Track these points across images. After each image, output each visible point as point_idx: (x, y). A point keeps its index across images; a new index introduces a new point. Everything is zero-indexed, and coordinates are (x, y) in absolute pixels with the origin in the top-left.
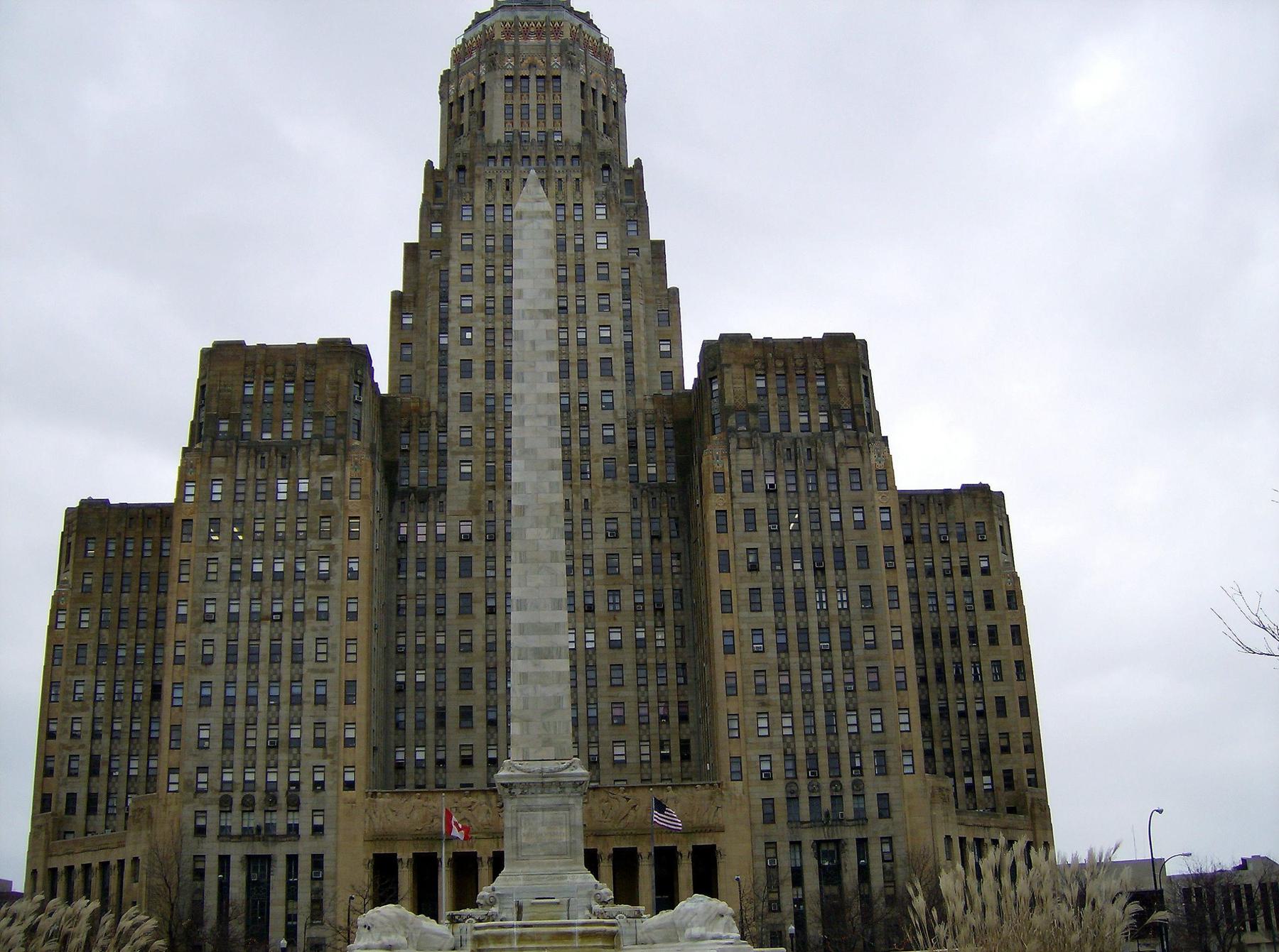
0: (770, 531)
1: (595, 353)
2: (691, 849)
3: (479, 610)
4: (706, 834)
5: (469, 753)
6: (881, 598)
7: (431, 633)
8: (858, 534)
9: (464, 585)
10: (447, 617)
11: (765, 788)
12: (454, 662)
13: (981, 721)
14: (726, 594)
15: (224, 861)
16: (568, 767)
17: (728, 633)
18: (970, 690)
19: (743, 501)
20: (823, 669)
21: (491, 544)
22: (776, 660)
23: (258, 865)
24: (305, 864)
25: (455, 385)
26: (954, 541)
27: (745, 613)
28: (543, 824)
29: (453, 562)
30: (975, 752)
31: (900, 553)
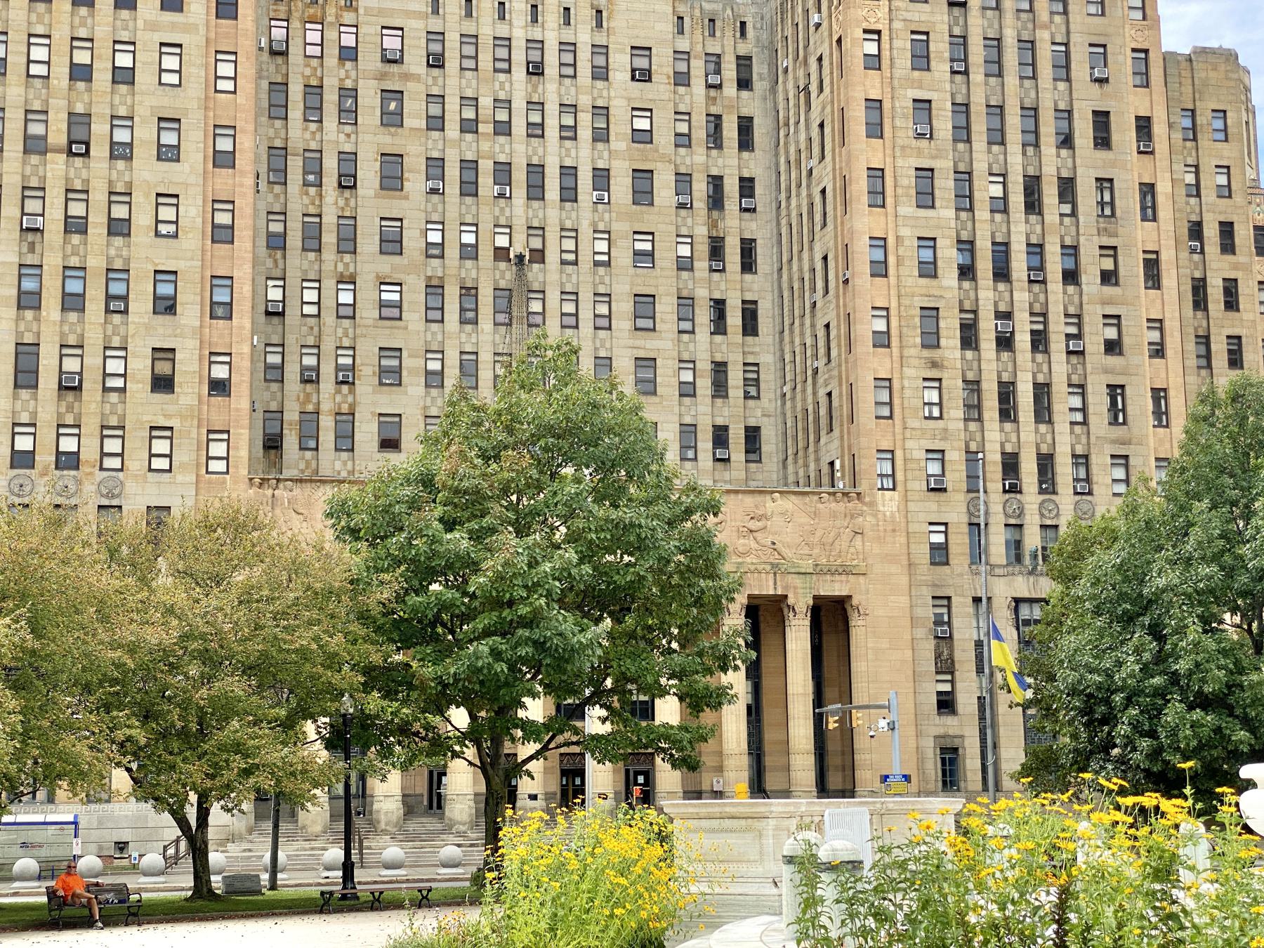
0: (954, 72)
2: (811, 602)
3: (416, 183)
4: (837, 577)
6: (1128, 201)
9: (389, 141)
10: (360, 191)
11: (934, 507)
14: (877, 174)
17: (880, 242)
19: (908, 16)
20: (1032, 314)
21: (436, 72)
22: (956, 292)
27: (908, 209)
29: (369, 99)
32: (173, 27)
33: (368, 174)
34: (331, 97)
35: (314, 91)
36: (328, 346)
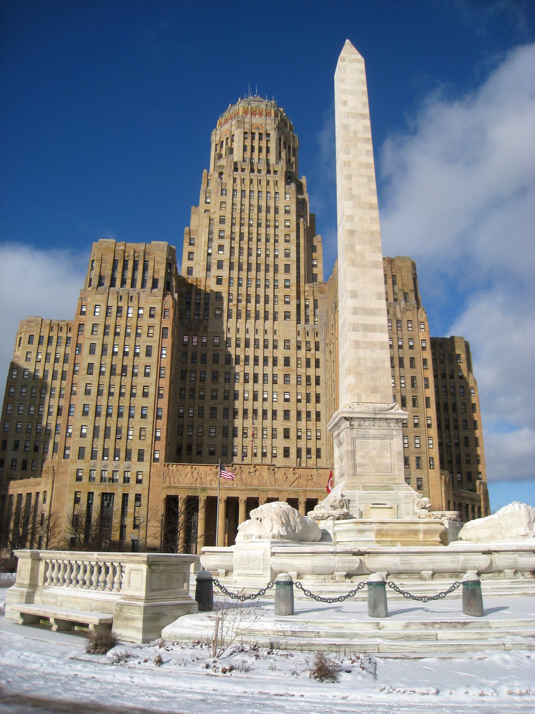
1: (282, 261)
5: (213, 449)
7: (197, 390)
8: (411, 351)
12: (208, 403)
13: (457, 448)
15: (90, 495)
16: (392, 408)
18: (453, 433)
23: (107, 497)
24: (131, 498)
25: (215, 272)
26: (446, 362)
28: (374, 449)
30: (454, 462)
31: (430, 363)
32: (150, 341)
33: (209, 377)
34: (199, 356)
35: (194, 355)
36: (195, 426)
